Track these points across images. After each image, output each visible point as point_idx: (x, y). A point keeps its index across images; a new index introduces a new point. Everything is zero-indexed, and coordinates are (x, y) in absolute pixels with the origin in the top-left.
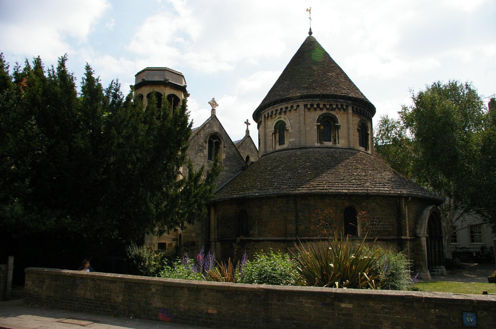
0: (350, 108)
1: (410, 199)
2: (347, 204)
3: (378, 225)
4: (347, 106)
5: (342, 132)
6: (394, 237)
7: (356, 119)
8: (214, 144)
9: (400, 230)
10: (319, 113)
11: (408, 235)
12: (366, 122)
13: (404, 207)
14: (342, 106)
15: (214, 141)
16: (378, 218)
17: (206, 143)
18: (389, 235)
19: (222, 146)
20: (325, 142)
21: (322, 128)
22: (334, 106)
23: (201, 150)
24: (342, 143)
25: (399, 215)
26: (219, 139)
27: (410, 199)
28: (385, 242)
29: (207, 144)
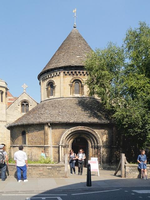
0: (62, 74)
1: (49, 124)
2: (23, 130)
3: (35, 139)
4: (60, 73)
5: (57, 89)
6: (43, 145)
7: (68, 78)
8: (25, 105)
9: (45, 140)
10: (48, 80)
11: (49, 144)
12: (80, 78)
13: (47, 129)
14: (57, 73)
15: (25, 104)
16: (35, 136)
17: (19, 105)
18: (40, 144)
19: (29, 105)
20: (50, 97)
21: (49, 89)
22: (52, 75)
23: (17, 109)
24: (57, 94)
25: (45, 134)
26: (28, 103)
27: (49, 124)
28: (38, 148)
29: (20, 106)
